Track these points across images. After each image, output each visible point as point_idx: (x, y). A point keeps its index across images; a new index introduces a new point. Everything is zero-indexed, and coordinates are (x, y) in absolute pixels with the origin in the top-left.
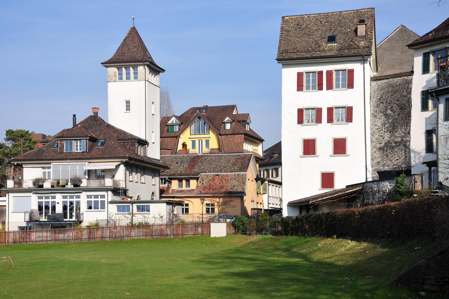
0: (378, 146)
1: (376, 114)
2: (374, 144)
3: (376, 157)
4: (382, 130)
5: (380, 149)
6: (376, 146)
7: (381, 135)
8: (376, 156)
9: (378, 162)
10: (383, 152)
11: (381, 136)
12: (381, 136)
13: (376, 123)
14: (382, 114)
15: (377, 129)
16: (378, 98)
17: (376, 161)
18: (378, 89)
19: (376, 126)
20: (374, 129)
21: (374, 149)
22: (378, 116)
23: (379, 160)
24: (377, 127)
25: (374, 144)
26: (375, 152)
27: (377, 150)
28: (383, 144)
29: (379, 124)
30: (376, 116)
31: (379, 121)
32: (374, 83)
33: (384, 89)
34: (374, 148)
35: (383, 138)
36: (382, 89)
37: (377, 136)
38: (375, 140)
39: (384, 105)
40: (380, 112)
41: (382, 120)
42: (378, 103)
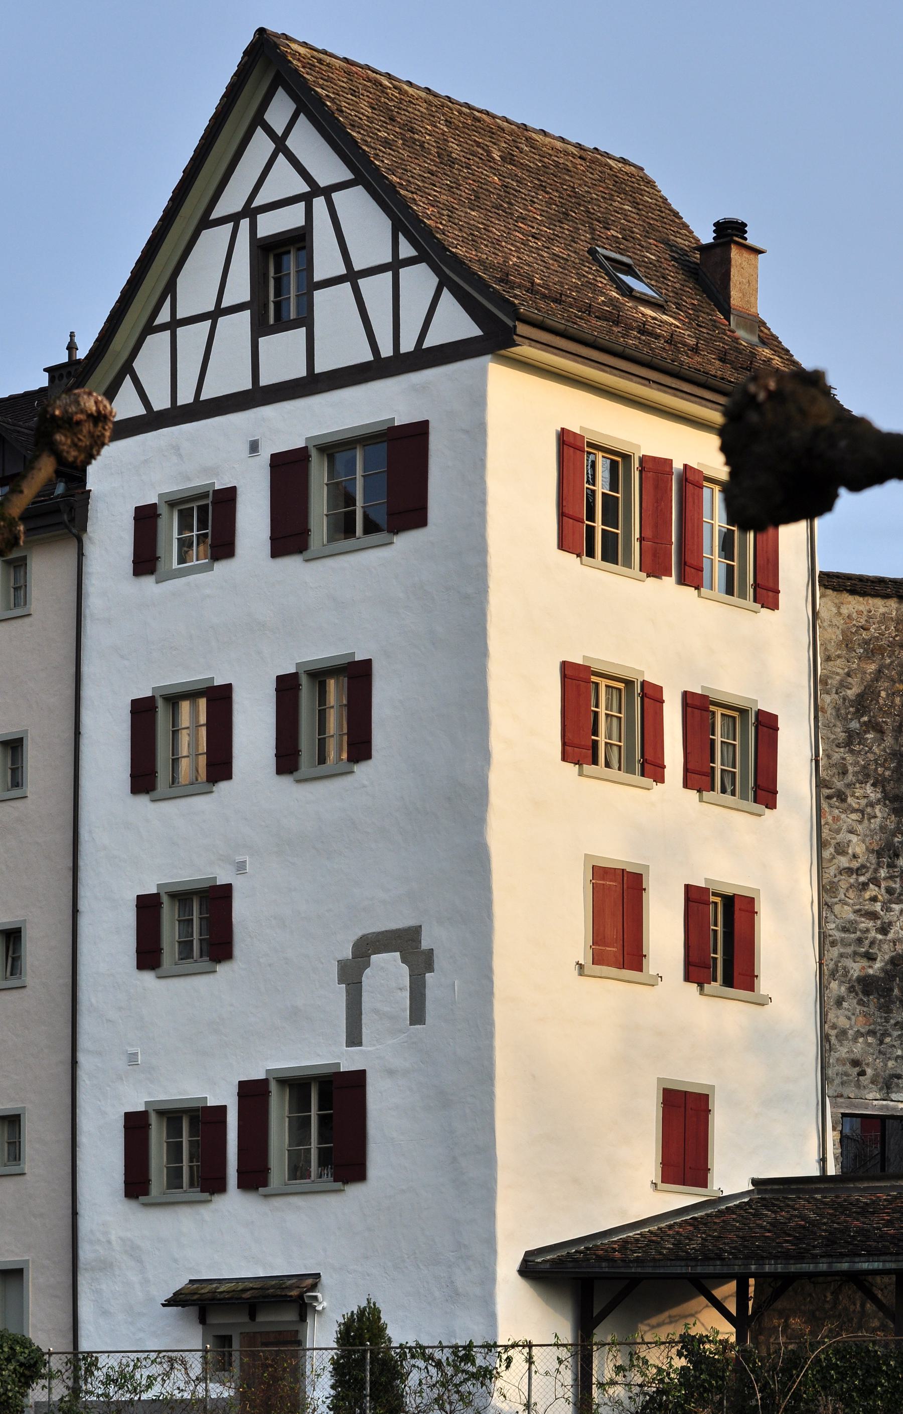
0: (856, 968)
1: (839, 784)
2: (835, 952)
3: (843, 1033)
4: (875, 881)
5: (866, 986)
6: (846, 971)
7: (868, 907)
8: (843, 1022)
9: (855, 1063)
10: (886, 1008)
11: (873, 916)
12: (873, 916)
13: (843, 836)
14: (874, 794)
15: (850, 871)
16: (850, 694)
17: (842, 1051)
18: (847, 643)
19: (841, 850)
20: (832, 871)
21: (834, 985)
22: (850, 800)
23: (858, 1048)
24: (844, 862)
25: (835, 952)
26: (839, 1002)
27: (851, 989)
28: (878, 965)
29: (857, 846)
30: (841, 797)
31: (859, 828)
32: (827, 604)
33: (881, 650)
34: (833, 974)
35: (884, 930)
36: (872, 650)
37: (847, 913)
38: (838, 935)
39: (889, 740)
40: (865, 775)
41: (876, 823)
42: (854, 725)
